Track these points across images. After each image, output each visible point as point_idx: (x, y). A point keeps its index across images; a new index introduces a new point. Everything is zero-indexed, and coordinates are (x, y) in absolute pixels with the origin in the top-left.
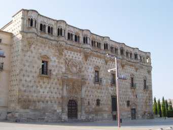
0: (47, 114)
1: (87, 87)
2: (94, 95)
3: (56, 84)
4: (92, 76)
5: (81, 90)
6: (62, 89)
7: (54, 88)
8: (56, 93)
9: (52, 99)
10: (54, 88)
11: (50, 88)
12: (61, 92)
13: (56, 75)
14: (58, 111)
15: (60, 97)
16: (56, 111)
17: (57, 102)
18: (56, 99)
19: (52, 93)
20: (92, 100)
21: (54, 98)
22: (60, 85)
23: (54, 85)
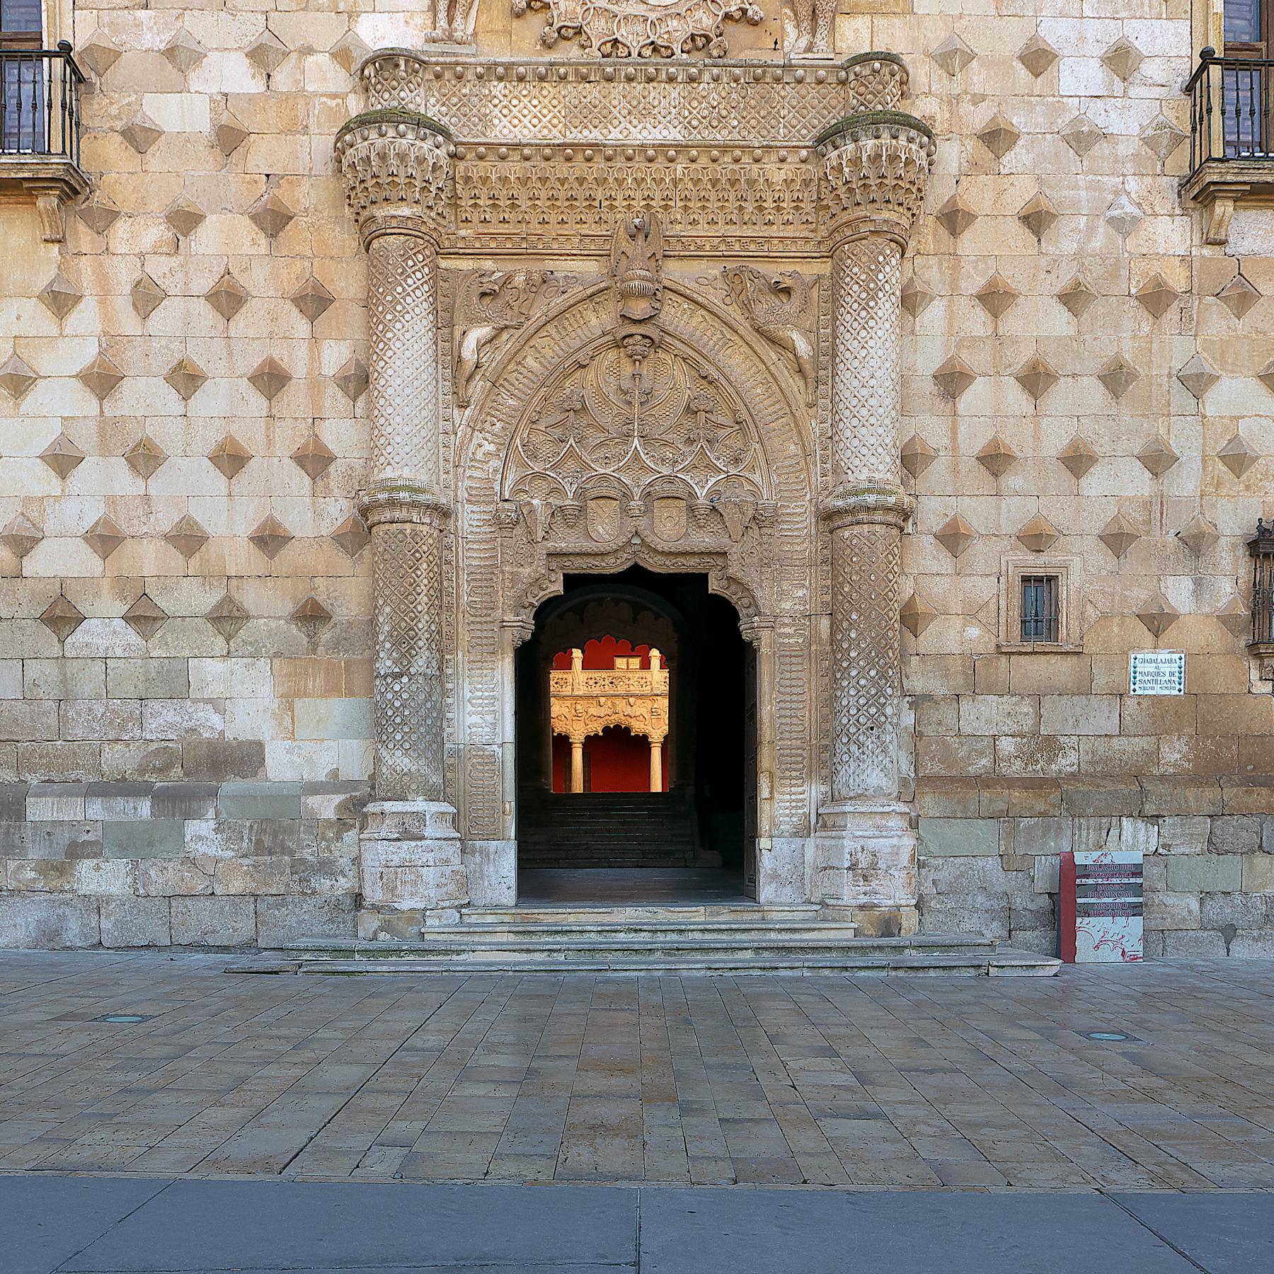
0: (40, 810)
1: (994, 299)
2: (1184, 439)
3: (228, 299)
4: (1121, 60)
5: (820, 372)
6: (359, 381)
7: (186, 379)
8: (231, 460)
9: (148, 558)
10: (186, 379)
11: (103, 381)
12: (340, 435)
13: (229, 140)
14: (283, 764)
15: (314, 515)
16: (247, 758)
17: (269, 605)
18: (238, 554)
19: (145, 458)
20: (1117, 541)
21: (188, 539)
22: (314, 302)
23: (183, 323)
